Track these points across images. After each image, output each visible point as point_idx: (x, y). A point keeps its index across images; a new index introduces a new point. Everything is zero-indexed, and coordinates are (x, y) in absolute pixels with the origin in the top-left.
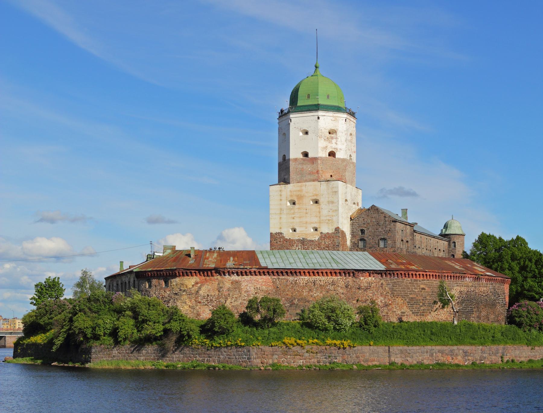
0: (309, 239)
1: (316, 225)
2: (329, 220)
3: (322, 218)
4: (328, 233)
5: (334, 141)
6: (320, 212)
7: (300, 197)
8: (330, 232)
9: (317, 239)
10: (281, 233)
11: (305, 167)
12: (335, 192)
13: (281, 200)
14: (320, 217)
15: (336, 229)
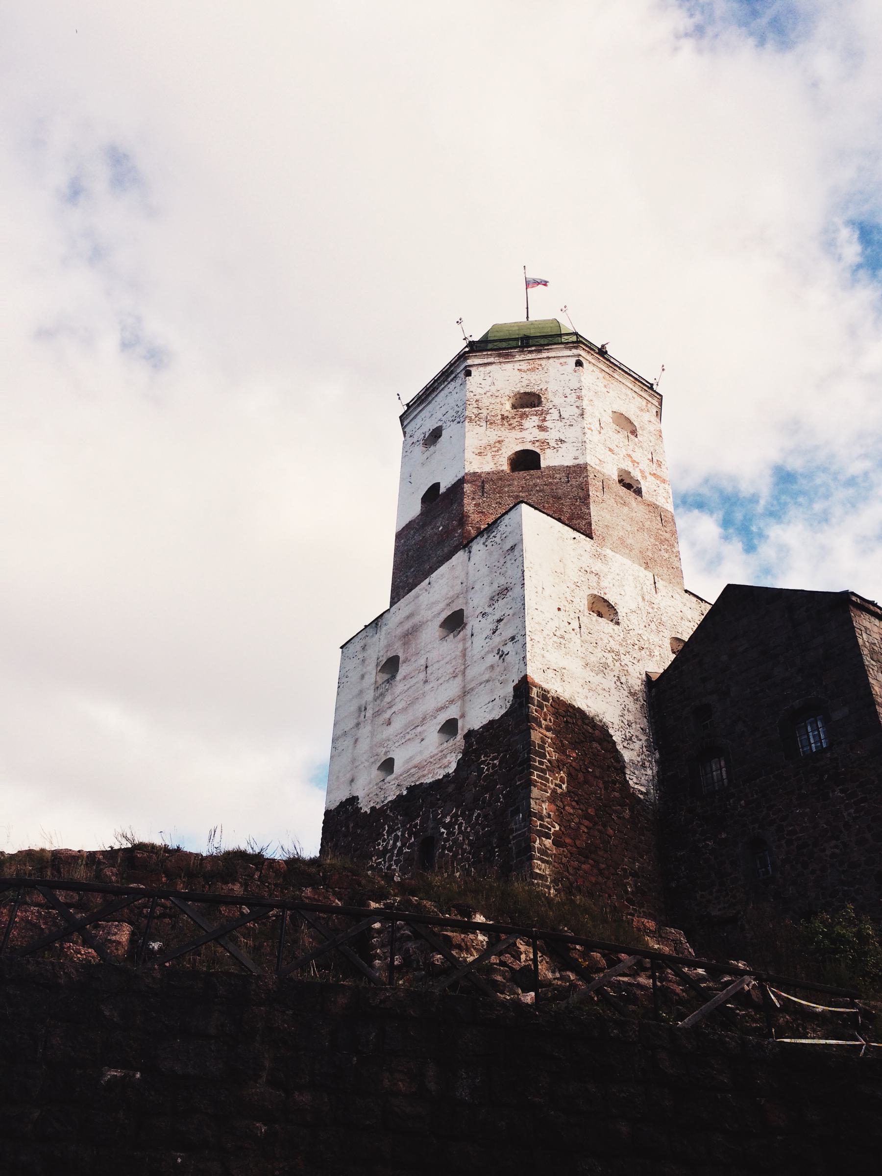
0: (428, 780)
1: (452, 712)
2: (492, 667)
3: (470, 673)
4: (491, 722)
5: (532, 422)
6: (464, 655)
7: (410, 635)
8: (497, 713)
9: (451, 770)
10: (353, 800)
11: (429, 531)
12: (512, 548)
13: (363, 677)
14: (464, 673)
15: (516, 688)
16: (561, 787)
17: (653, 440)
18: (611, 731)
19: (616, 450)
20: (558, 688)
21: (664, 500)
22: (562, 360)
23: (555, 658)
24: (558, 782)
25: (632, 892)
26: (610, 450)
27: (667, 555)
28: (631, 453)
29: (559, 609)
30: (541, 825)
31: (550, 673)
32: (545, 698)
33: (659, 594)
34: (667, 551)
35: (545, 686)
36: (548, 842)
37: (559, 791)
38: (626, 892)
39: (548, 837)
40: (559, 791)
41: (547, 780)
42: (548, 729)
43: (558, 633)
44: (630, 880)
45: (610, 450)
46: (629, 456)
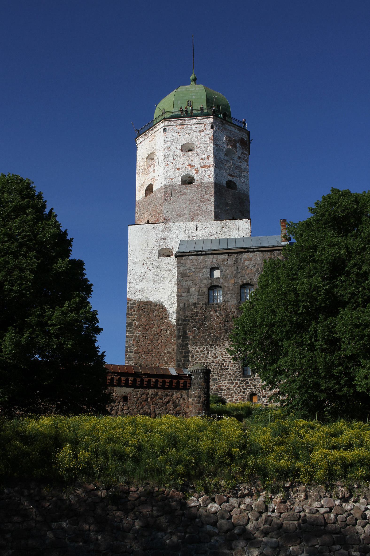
16: (138, 334)
17: (205, 145)
18: (164, 304)
19: (181, 166)
20: (140, 297)
21: (208, 177)
22: (160, 130)
23: (140, 286)
24: (137, 332)
25: (167, 359)
26: (178, 169)
27: (205, 207)
28: (190, 163)
29: (143, 264)
30: (129, 349)
31: (138, 293)
32: (134, 303)
33: (198, 230)
34: (205, 205)
35: (134, 299)
36: (131, 354)
37: (137, 335)
38: (165, 360)
39: (131, 352)
40: (137, 335)
41: (133, 333)
42: (135, 314)
43: (142, 275)
44: (167, 355)
45: (178, 169)
46: (190, 165)
